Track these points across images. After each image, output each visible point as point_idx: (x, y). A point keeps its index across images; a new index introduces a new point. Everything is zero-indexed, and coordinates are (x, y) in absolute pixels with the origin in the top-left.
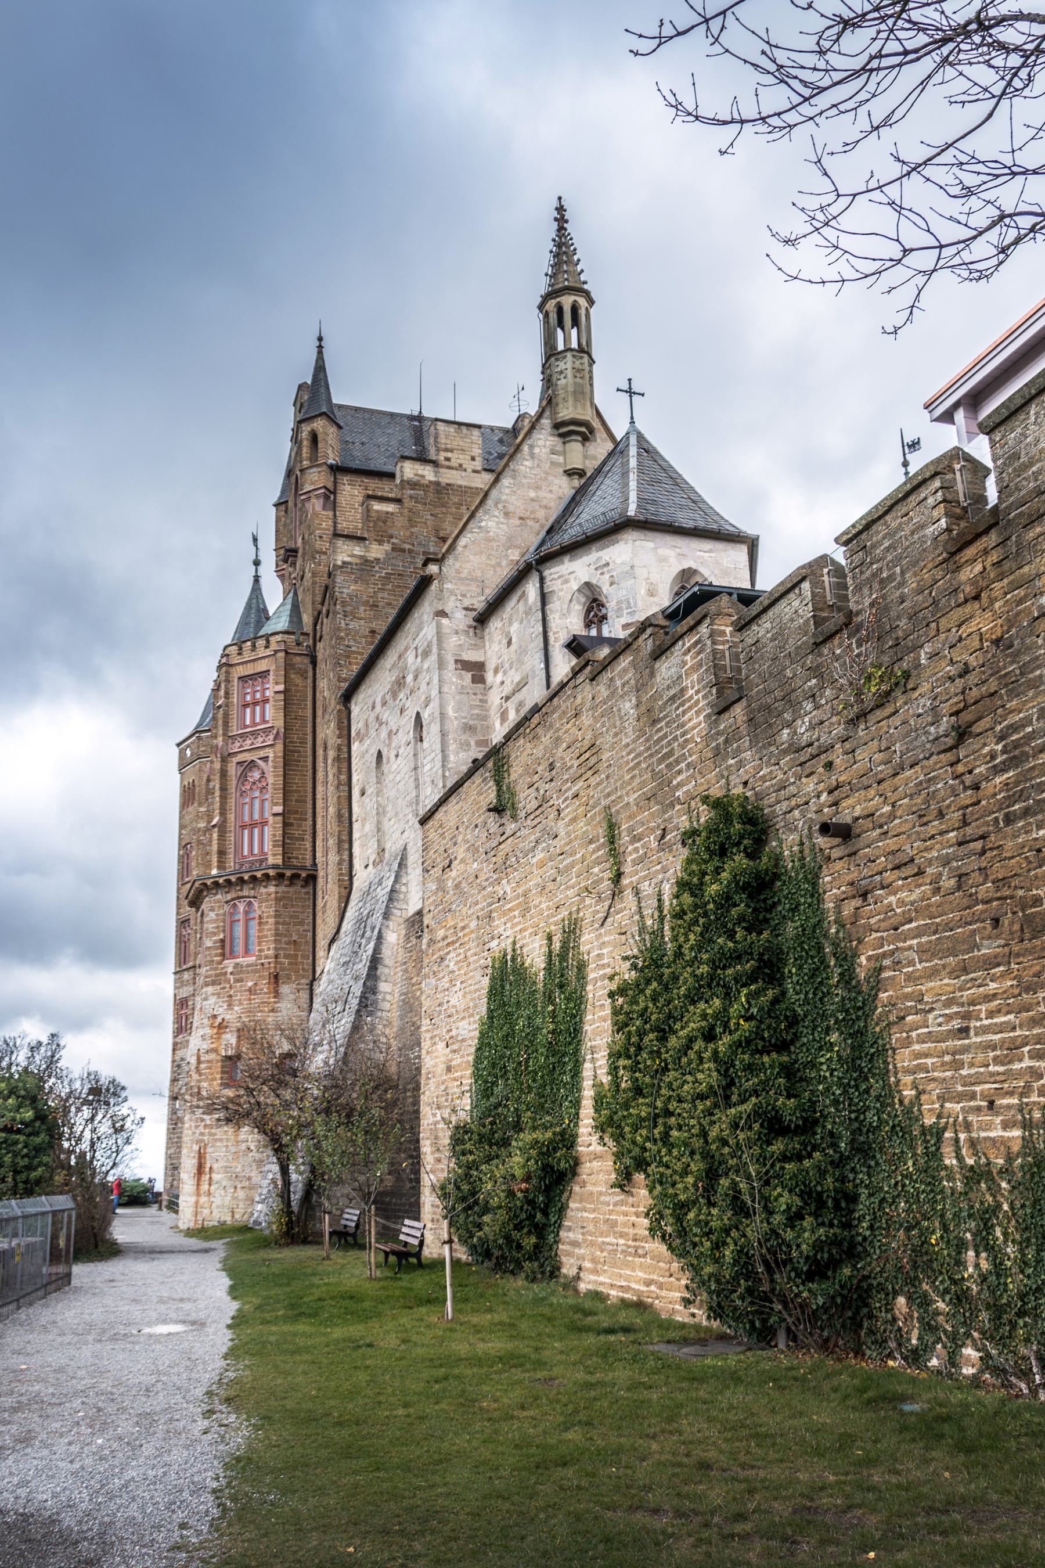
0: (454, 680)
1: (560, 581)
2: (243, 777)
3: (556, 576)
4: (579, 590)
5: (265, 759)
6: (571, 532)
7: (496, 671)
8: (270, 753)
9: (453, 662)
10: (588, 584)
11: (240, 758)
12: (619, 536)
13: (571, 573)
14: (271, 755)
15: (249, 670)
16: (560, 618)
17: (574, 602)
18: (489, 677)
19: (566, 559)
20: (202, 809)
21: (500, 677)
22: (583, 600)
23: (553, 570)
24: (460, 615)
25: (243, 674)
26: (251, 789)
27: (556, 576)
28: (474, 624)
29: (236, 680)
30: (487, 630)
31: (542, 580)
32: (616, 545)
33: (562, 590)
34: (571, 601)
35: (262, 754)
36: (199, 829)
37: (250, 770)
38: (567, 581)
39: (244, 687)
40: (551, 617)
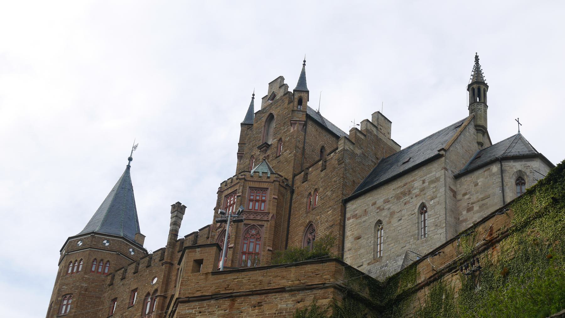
0: (449, 193)
1: (509, 167)
2: (247, 232)
3: (507, 165)
4: (516, 172)
5: (262, 226)
6: (479, 162)
7: (465, 194)
8: (265, 224)
9: (448, 186)
10: (520, 170)
11: (245, 222)
12: (534, 159)
13: (514, 166)
14: (266, 225)
15: (256, 185)
16: (509, 179)
17: (514, 175)
18: (459, 197)
19: (512, 161)
20: (86, 276)
21: (467, 197)
22: (516, 176)
23: (506, 163)
24: (450, 172)
25: (252, 186)
26: (250, 237)
27: (507, 165)
28: (454, 177)
29: (248, 187)
30: (459, 181)
31: (501, 165)
32: (533, 162)
33: (510, 170)
34: (513, 174)
35: (260, 223)
36: (82, 287)
37: (251, 229)
38: (512, 168)
39: (251, 192)
40: (504, 178)
